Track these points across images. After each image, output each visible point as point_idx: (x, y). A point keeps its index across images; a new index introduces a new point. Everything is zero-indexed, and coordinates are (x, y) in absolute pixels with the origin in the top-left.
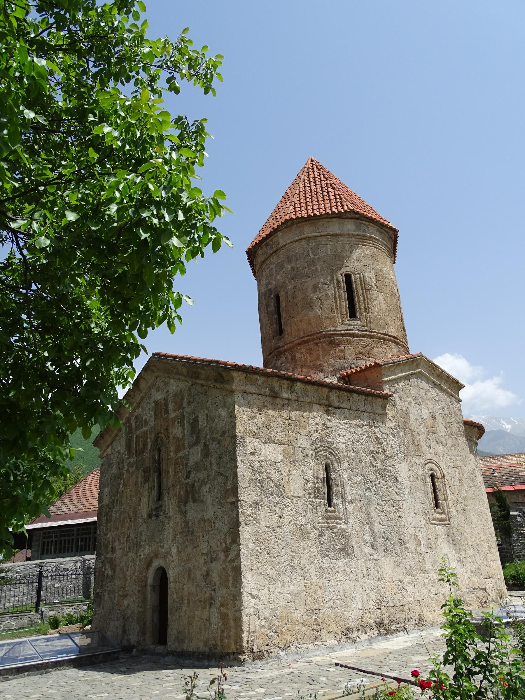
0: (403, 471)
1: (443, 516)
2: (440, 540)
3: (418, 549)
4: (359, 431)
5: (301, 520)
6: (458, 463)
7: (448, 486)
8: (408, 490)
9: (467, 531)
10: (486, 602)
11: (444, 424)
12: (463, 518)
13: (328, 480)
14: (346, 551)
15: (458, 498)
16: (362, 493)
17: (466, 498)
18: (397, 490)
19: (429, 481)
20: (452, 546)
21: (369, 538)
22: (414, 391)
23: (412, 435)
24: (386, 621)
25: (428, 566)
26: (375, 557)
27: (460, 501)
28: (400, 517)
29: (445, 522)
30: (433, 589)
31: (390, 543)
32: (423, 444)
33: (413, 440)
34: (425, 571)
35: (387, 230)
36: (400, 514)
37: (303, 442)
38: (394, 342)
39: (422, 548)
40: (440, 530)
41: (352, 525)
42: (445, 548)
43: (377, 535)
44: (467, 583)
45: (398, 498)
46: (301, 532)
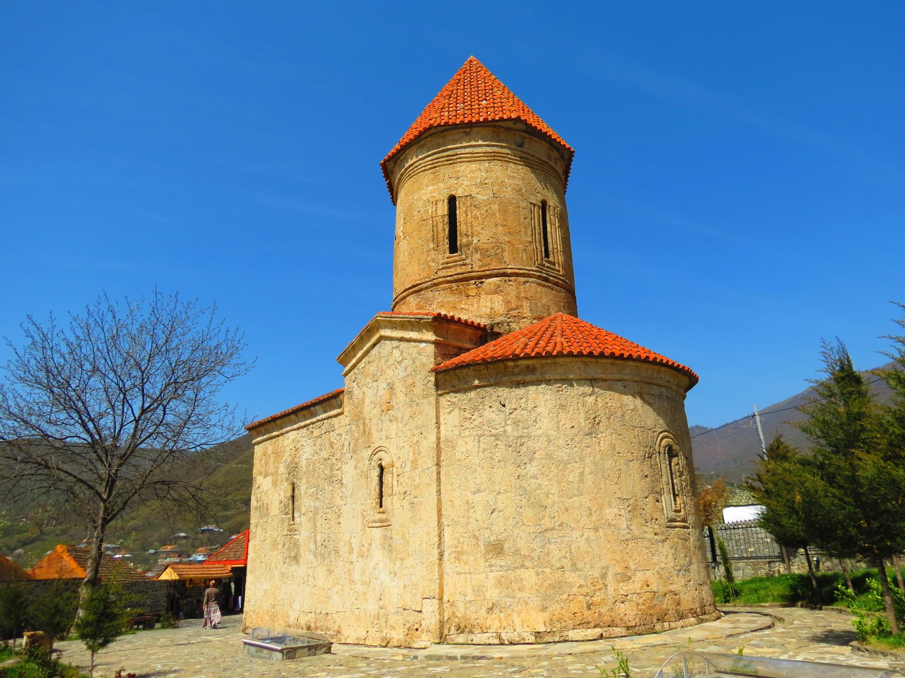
0: (349, 472)
1: (384, 516)
2: (374, 546)
3: (350, 557)
4: (319, 441)
5: (275, 536)
6: (415, 439)
7: (395, 476)
8: (350, 492)
9: (411, 532)
10: (417, 630)
11: (404, 390)
12: (410, 515)
13: (293, 497)
14: (296, 559)
15: (406, 489)
16: (313, 504)
17: (417, 487)
18: (341, 494)
19: (375, 473)
20: (386, 553)
21: (312, 547)
22: (372, 368)
23: (364, 423)
24: (313, 625)
25: (357, 577)
26: (315, 564)
27: (408, 493)
28: (339, 523)
29: (385, 524)
30: (356, 602)
31: (327, 551)
32: (374, 430)
33: (364, 430)
34: (352, 582)
35: (427, 134)
36: (340, 520)
37: (282, 469)
38: (415, 292)
39: (354, 557)
40: (378, 533)
41: (303, 536)
42: (378, 555)
43: (319, 544)
44: (396, 600)
45: (342, 503)
46: (275, 544)
